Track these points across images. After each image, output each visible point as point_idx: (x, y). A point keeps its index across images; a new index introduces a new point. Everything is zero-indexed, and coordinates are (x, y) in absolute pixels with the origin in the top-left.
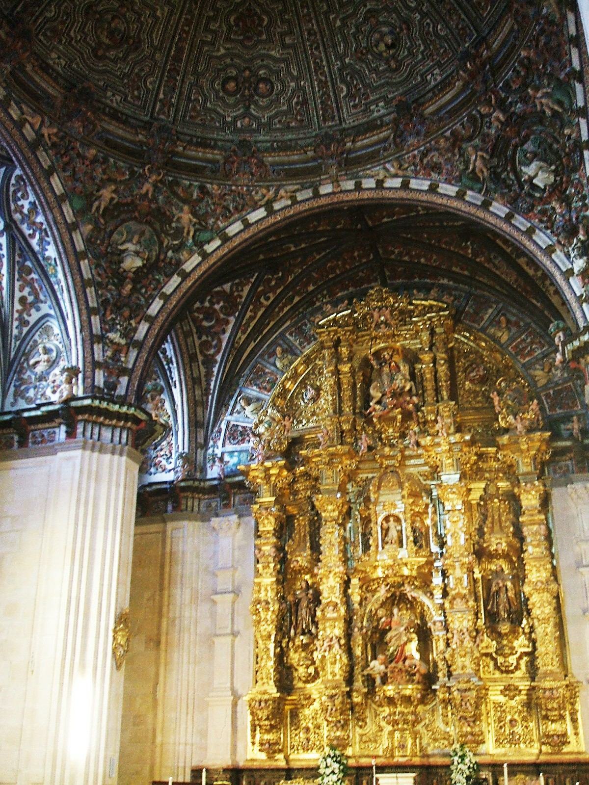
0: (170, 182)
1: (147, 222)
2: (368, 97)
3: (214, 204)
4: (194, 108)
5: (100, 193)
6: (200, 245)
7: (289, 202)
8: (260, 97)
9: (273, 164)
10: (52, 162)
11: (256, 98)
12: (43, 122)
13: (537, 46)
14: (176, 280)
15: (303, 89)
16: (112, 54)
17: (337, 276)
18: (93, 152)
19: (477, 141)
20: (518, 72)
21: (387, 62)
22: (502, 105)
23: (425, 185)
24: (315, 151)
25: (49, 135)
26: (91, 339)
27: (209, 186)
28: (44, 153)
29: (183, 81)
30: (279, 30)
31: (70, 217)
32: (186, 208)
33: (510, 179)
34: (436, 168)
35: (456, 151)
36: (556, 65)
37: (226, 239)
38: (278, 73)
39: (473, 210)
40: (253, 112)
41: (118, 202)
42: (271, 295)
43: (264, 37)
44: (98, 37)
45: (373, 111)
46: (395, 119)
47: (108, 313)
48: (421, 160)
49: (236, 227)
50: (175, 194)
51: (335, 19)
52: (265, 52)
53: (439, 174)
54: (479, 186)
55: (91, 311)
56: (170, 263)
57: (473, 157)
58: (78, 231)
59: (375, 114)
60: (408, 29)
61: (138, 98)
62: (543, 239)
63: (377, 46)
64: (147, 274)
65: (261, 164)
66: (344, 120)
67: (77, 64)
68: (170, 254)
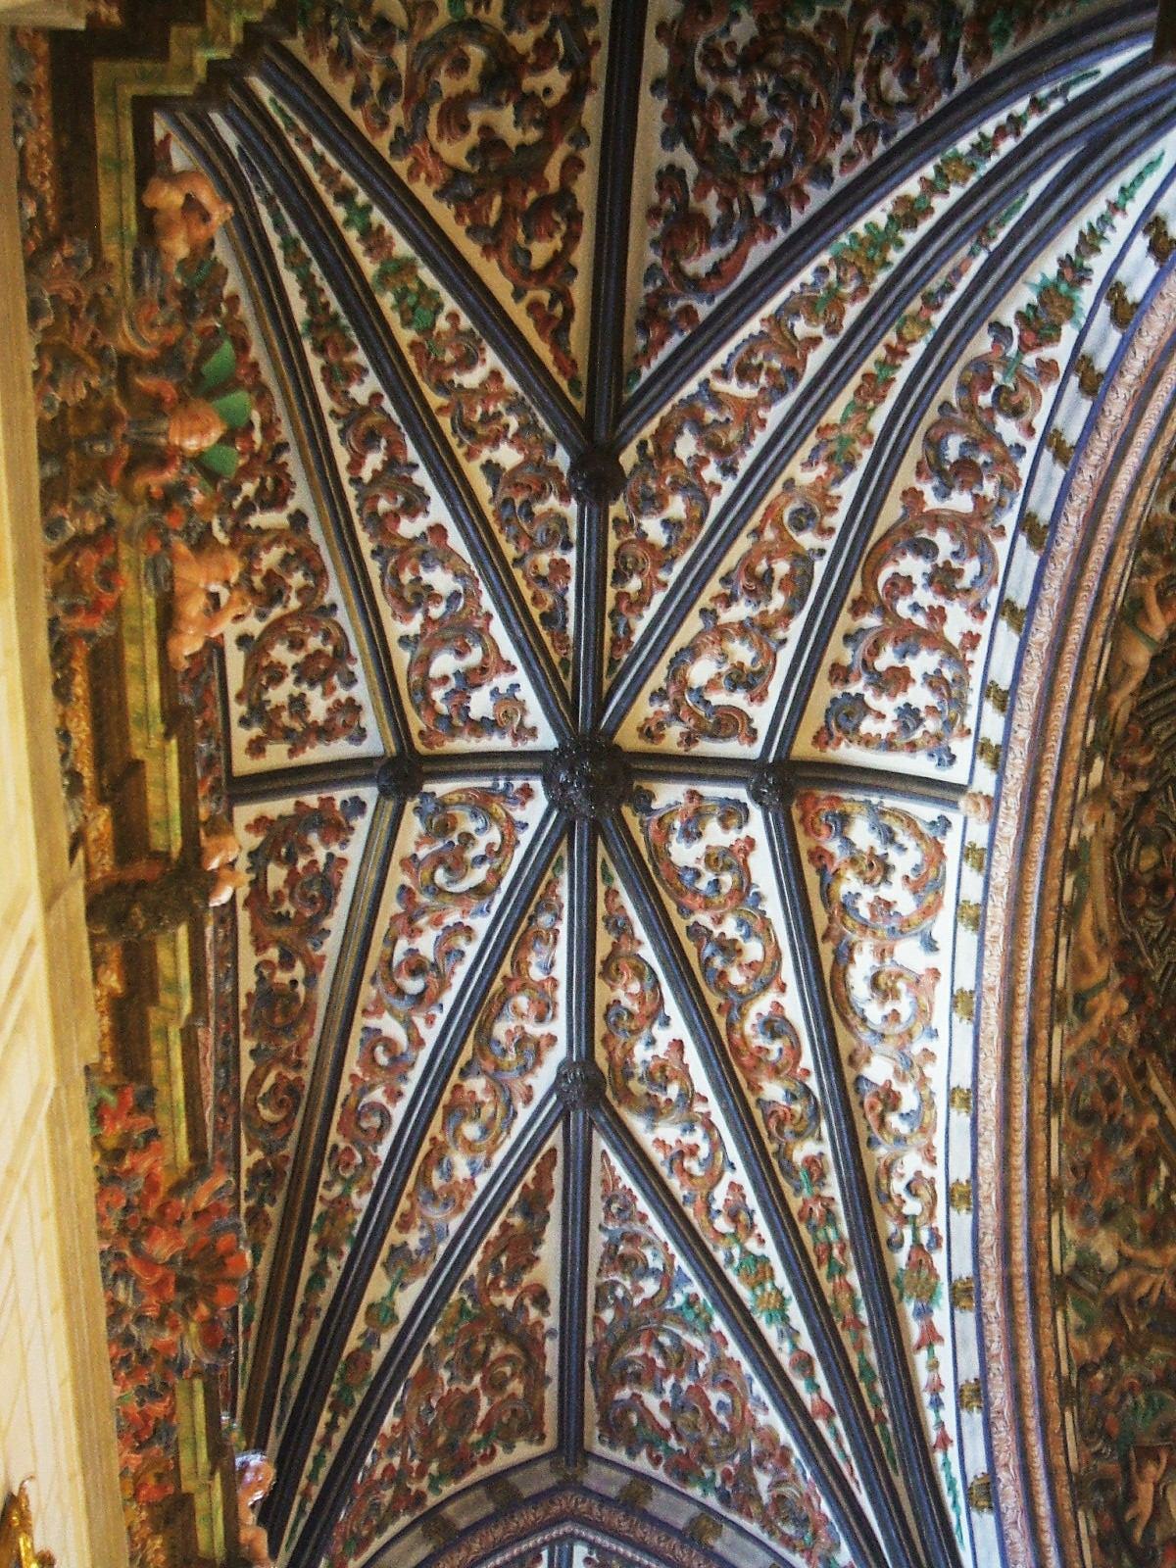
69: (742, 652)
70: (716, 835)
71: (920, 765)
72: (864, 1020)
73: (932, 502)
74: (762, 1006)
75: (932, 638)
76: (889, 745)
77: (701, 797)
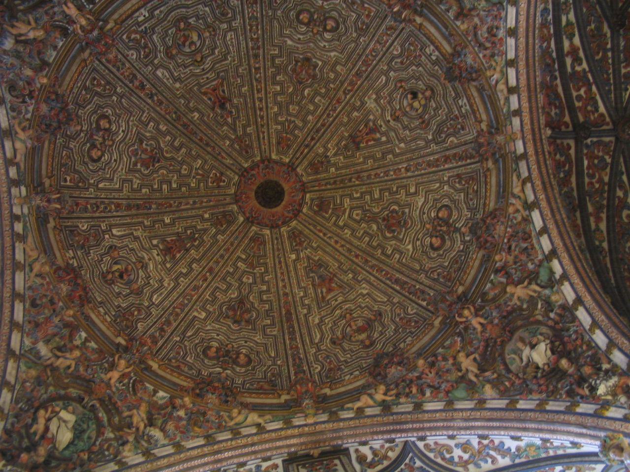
0: (483, 301)
1: (512, 333)
2: (456, 116)
5: (464, 368)
7: (529, 185)
9: (496, 203)
11: (451, 221)
16: (376, 335)
23: (511, 42)
25: (385, 394)
28: (399, 406)
29: (421, 283)
30: (404, 197)
32: (509, 289)
34: (491, 32)
37: (554, 253)
38: (435, 200)
41: (480, 355)
43: (407, 210)
44: (357, 341)
45: (466, 110)
47: (580, 391)
48: (486, 49)
50: (494, 300)
51: (399, 148)
53: (497, 28)
56: (560, 315)
60: (401, 81)
64: (563, 344)
68: (552, 315)
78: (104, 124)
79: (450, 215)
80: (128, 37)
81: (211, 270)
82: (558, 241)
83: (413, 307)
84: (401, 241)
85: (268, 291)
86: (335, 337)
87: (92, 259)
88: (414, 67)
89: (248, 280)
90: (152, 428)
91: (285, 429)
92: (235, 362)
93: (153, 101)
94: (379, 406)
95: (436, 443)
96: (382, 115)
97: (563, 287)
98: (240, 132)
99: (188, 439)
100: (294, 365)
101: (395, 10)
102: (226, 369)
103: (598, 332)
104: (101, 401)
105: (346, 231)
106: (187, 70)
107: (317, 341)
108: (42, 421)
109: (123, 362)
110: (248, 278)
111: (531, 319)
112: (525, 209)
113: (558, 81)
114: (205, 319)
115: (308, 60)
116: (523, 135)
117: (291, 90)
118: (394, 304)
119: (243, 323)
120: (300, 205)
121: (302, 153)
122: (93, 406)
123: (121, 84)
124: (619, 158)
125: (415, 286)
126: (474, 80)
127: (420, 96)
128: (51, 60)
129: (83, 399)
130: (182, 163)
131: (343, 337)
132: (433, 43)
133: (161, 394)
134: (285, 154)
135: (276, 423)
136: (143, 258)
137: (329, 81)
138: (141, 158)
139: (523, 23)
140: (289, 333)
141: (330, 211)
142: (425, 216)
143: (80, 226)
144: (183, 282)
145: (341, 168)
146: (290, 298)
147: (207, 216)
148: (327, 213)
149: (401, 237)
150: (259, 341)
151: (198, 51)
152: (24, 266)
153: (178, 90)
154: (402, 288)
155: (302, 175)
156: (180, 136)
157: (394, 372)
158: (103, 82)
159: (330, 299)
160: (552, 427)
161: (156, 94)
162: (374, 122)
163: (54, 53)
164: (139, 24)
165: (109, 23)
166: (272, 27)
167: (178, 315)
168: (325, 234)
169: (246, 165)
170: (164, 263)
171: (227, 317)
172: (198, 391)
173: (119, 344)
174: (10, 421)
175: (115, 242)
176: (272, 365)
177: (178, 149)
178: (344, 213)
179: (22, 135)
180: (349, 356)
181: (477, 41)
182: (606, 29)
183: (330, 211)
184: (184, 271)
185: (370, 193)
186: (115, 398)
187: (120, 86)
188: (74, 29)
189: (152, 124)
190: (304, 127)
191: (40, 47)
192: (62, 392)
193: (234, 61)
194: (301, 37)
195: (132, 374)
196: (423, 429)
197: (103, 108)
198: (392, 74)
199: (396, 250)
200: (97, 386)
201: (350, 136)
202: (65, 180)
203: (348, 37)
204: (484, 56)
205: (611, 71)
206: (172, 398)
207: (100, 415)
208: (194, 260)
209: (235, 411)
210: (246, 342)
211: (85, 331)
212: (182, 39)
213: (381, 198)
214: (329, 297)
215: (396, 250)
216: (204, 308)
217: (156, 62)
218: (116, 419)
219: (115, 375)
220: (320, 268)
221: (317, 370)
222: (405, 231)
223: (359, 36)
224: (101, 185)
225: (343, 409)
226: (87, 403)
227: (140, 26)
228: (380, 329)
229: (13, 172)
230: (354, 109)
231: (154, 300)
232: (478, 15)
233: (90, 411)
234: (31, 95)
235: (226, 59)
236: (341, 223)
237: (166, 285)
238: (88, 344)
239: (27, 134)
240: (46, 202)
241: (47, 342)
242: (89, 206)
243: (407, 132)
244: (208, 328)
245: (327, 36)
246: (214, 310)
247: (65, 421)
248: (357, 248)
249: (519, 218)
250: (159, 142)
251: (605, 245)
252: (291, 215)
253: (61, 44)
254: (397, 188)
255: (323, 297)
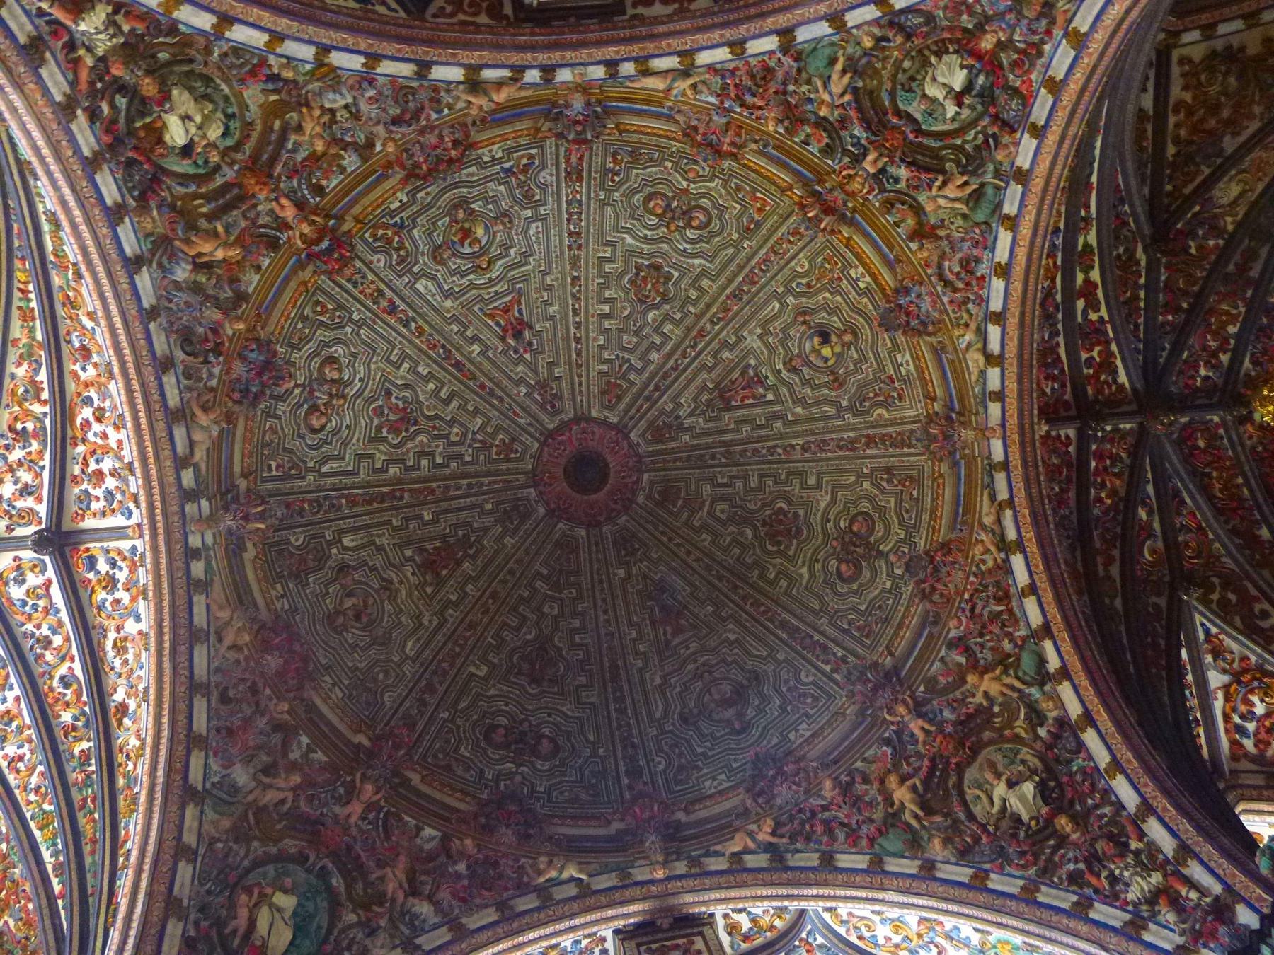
1: (975, 752)
2: (890, 378)
3: (981, 635)
4: (859, 629)
5: (896, 802)
6: (1043, 677)
7: (1008, 513)
8: (871, 534)
9: (952, 528)
10: (817, 851)
11: (872, 539)
12: (751, 834)
13: (760, 108)
14: (1090, 738)
15: (873, 470)
16: (751, 713)
17: (1247, 483)
18: (828, 784)
19: (922, 198)
20: (808, 135)
21: (847, 346)
22: (857, 160)
23: (998, 285)
24: (941, 460)
25: (773, 834)
26: (1131, 938)
27: (952, 634)
28: (797, 856)
29: (822, 633)
30: (797, 491)
31: (909, 866)
32: (971, 679)
33: (975, 138)
34: (968, 265)
35: (941, 233)
36: (780, 75)
37: (1047, 630)
39: (1033, 200)
40: (888, 548)
41: (922, 782)
42: (1257, 608)
43: (801, 512)
45: (908, 371)
46: (904, 333)
47: (1094, 881)
48: (956, 290)
49: (1031, 605)
51: (793, 414)
52: (819, 514)
53: (978, 260)
54: (990, 191)
55: (1081, 910)
57: (941, 202)
58: (939, 865)
59: (912, 367)
60: (804, 313)
61: (816, 699)
62: (1061, 58)
63: (826, 360)
65: (946, 547)
66: (918, 416)
67: (736, 760)
68: (1042, 732)
69: (26, 476)
70: (33, 580)
71: (118, 521)
72: (112, 669)
73: (83, 376)
74: (63, 670)
75: (107, 450)
76: (103, 514)
77: (20, 559)
78: (330, 373)
79: (871, 530)
80: (374, 236)
81: (494, 596)
82: (1053, 611)
83: (809, 671)
84: (791, 560)
85: (582, 629)
86: (686, 710)
87: (312, 593)
88: (827, 295)
89: (551, 610)
90: (416, 901)
91: (621, 887)
92: (535, 752)
93: (410, 330)
94: (765, 851)
95: (850, 914)
96: (771, 362)
97: (1060, 688)
98: (544, 373)
99: (470, 912)
100: (624, 758)
101: (810, 215)
102: (521, 765)
103: (1120, 777)
104: (334, 856)
105: (704, 536)
106: (464, 280)
107: (658, 715)
108: (243, 913)
109: (369, 787)
110: (552, 607)
111: (1007, 732)
112: (1000, 550)
113: (1061, 339)
114: (486, 679)
115: (657, 267)
116: (1005, 432)
117: (626, 313)
118: (779, 663)
119: (545, 684)
120: (634, 492)
121: (638, 411)
122: (323, 868)
123: (359, 306)
124: (1143, 459)
125: (812, 637)
126: (930, 335)
127: (834, 338)
128: (251, 290)
129: (307, 858)
130: (453, 422)
131: (700, 713)
132: (864, 264)
133: (428, 831)
134: (611, 408)
135: (605, 876)
136: (390, 582)
137: (688, 301)
138: (388, 420)
139: (1021, 259)
140: (616, 700)
141: (680, 503)
142: (830, 525)
143: (293, 540)
144: (451, 616)
145: (699, 436)
146: (616, 643)
147: (489, 506)
148: (675, 506)
149: (791, 553)
150: (569, 713)
151: (484, 251)
152: (208, 633)
153: (448, 311)
154: (790, 636)
155: (638, 444)
156: (450, 382)
157: (784, 794)
158: (330, 307)
159: (677, 646)
160: (1047, 933)
161: (414, 319)
162: (756, 368)
163: (256, 278)
164: (392, 214)
165: (345, 221)
166: (602, 216)
167: (445, 673)
168: (670, 540)
169: (551, 426)
170: (421, 586)
171: (520, 673)
172: (483, 820)
173: (359, 746)
174: (192, 917)
175: (348, 558)
176: (591, 757)
177: (447, 402)
178: (701, 508)
179: (203, 419)
180: (708, 744)
181: (941, 277)
182: (1140, 254)
183: (680, 503)
184: (453, 598)
185: (745, 477)
186: (358, 848)
187: (358, 310)
188: (289, 238)
189: (406, 365)
190: (644, 368)
191: (232, 271)
192: (274, 850)
193: (540, 266)
194: (649, 233)
195: (382, 803)
196: (834, 898)
197: (330, 347)
198: (790, 300)
199: (782, 573)
200: (329, 833)
201: (717, 385)
202: (270, 469)
203: (724, 239)
204: (951, 302)
205: (1141, 320)
206: (446, 839)
207: (334, 882)
208: (468, 579)
209: (543, 859)
210: (549, 715)
211: (308, 736)
212: (459, 236)
213: (761, 489)
214: (677, 641)
215: (782, 573)
216: (484, 660)
217: (416, 269)
218: (359, 886)
219: (356, 808)
220: (664, 592)
221: (661, 767)
222: (798, 545)
223: (742, 238)
224: (325, 469)
225: (707, 855)
226: (314, 864)
227: (392, 218)
228: (757, 702)
229: (188, 477)
230: (725, 345)
231: (407, 651)
232: (948, 236)
233: (318, 876)
234: (217, 351)
235: (526, 264)
236: (697, 523)
237: (426, 623)
238: (312, 755)
239: (212, 416)
240: (242, 518)
241: (248, 761)
242: (306, 505)
243: (809, 391)
244: (492, 692)
245: (690, 234)
246: (500, 660)
247: (279, 910)
248: (719, 563)
249: (990, 564)
250: (416, 393)
251: (1118, 603)
252: (619, 507)
253: (267, 261)
254: (788, 474)
255: (668, 643)
